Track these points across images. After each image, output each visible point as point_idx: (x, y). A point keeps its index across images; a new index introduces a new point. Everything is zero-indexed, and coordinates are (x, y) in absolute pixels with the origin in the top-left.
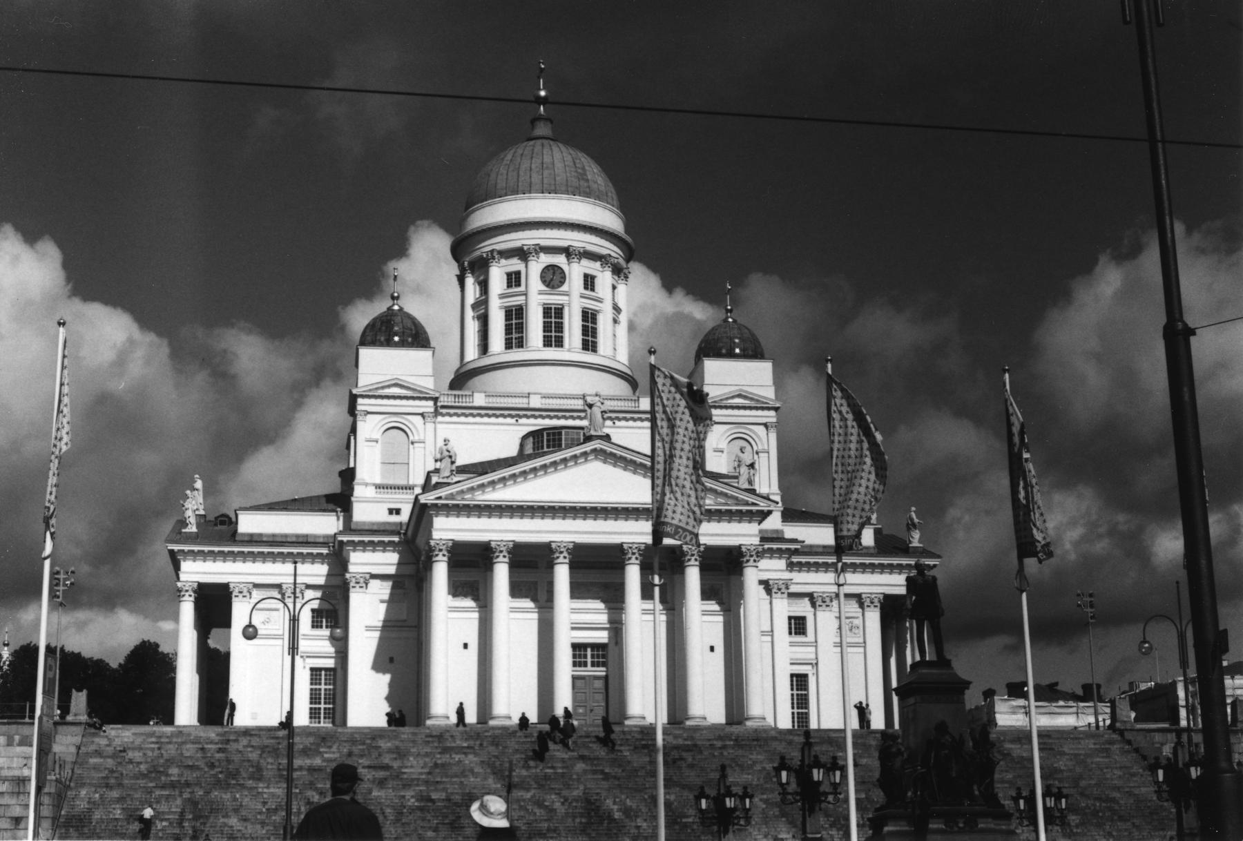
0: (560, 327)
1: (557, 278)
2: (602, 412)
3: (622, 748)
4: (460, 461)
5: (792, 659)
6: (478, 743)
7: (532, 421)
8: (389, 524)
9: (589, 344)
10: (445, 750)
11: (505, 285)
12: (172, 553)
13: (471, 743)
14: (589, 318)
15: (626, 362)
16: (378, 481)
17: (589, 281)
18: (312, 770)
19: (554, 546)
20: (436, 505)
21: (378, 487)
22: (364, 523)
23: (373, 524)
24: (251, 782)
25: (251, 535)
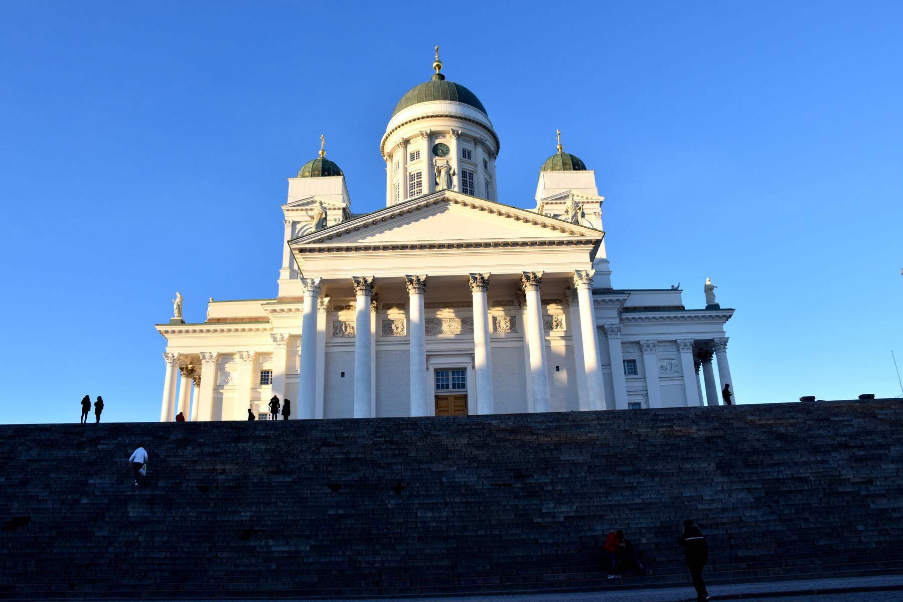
3: (441, 433)
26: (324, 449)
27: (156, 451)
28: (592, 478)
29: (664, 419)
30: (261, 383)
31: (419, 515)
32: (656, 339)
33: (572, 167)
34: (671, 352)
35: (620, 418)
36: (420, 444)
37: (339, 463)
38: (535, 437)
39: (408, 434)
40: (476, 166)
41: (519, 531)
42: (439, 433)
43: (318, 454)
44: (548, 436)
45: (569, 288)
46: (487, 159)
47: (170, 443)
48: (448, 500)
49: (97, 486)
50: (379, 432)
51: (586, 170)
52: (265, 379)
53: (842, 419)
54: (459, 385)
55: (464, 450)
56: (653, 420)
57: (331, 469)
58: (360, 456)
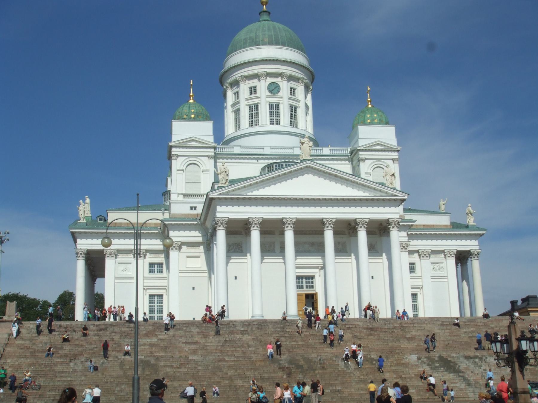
0: (278, 115)
1: (277, 89)
2: (309, 147)
4: (231, 177)
5: (411, 286)
6: (250, 328)
7: (267, 161)
8: (191, 214)
9: (294, 123)
10: (231, 332)
11: (249, 93)
12: (73, 233)
13: (246, 328)
14: (293, 109)
15: (312, 133)
16: (184, 192)
17: (293, 91)
18: (151, 345)
19: (284, 220)
20: (219, 198)
21: (185, 195)
22: (177, 214)
23: (182, 215)
24: (114, 353)
29: (447, 325)
30: (150, 272)
32: (430, 249)
33: (379, 122)
49: (196, 360)
51: (389, 124)
52: (152, 270)
54: (310, 286)
56: (441, 325)
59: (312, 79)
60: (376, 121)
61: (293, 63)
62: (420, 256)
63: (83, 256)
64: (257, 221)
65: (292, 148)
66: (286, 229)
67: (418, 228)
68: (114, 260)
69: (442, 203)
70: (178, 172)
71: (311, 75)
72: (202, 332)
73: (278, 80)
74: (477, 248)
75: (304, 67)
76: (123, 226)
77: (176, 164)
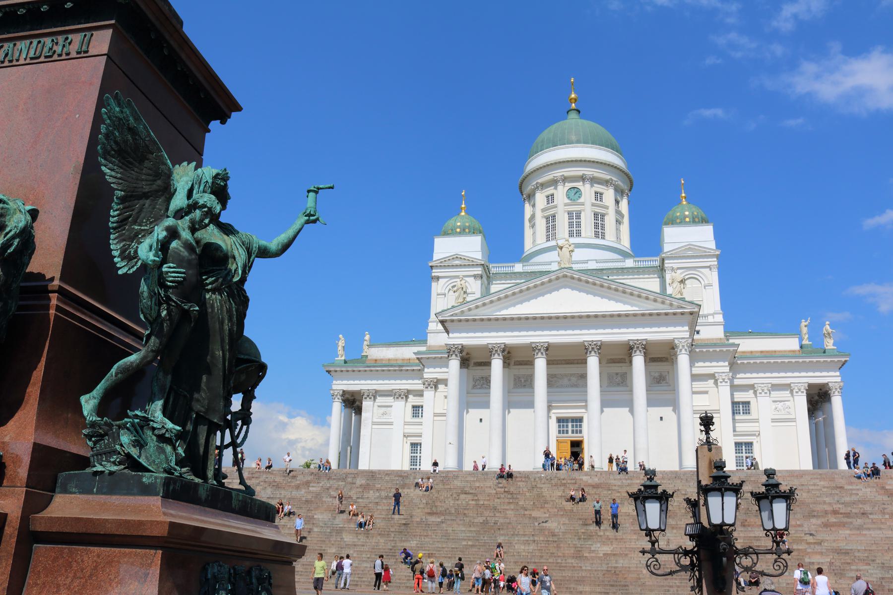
0: (579, 225)
14: (599, 218)
17: (599, 196)
19: (533, 346)
25: (376, 360)
26: (463, 496)
27: (349, 494)
28: (632, 528)
30: (413, 416)
31: (516, 547)
34: (786, 394)
35: (679, 478)
36: (528, 494)
37: (472, 508)
38: (610, 492)
39: (521, 486)
40: (608, 209)
41: (573, 561)
42: (543, 486)
43: (458, 500)
44: (619, 492)
45: (673, 348)
46: (619, 199)
47: (357, 488)
48: (536, 538)
50: (501, 483)
53: (854, 487)
55: (557, 501)
57: (466, 512)
58: (486, 503)
59: (628, 181)
60: (687, 220)
61: (597, 162)
62: (755, 392)
63: (338, 398)
64: (499, 347)
65: (586, 262)
66: (536, 357)
67: (751, 355)
68: (372, 403)
69: (804, 323)
70: (438, 296)
71: (627, 179)
72: (368, 485)
73: (579, 185)
74: (839, 380)
75: (612, 166)
76: (384, 362)
77: (437, 288)
